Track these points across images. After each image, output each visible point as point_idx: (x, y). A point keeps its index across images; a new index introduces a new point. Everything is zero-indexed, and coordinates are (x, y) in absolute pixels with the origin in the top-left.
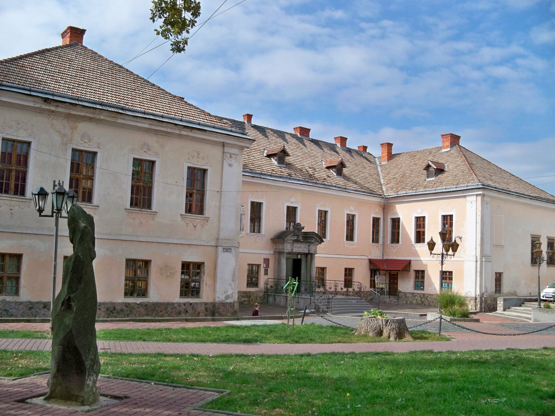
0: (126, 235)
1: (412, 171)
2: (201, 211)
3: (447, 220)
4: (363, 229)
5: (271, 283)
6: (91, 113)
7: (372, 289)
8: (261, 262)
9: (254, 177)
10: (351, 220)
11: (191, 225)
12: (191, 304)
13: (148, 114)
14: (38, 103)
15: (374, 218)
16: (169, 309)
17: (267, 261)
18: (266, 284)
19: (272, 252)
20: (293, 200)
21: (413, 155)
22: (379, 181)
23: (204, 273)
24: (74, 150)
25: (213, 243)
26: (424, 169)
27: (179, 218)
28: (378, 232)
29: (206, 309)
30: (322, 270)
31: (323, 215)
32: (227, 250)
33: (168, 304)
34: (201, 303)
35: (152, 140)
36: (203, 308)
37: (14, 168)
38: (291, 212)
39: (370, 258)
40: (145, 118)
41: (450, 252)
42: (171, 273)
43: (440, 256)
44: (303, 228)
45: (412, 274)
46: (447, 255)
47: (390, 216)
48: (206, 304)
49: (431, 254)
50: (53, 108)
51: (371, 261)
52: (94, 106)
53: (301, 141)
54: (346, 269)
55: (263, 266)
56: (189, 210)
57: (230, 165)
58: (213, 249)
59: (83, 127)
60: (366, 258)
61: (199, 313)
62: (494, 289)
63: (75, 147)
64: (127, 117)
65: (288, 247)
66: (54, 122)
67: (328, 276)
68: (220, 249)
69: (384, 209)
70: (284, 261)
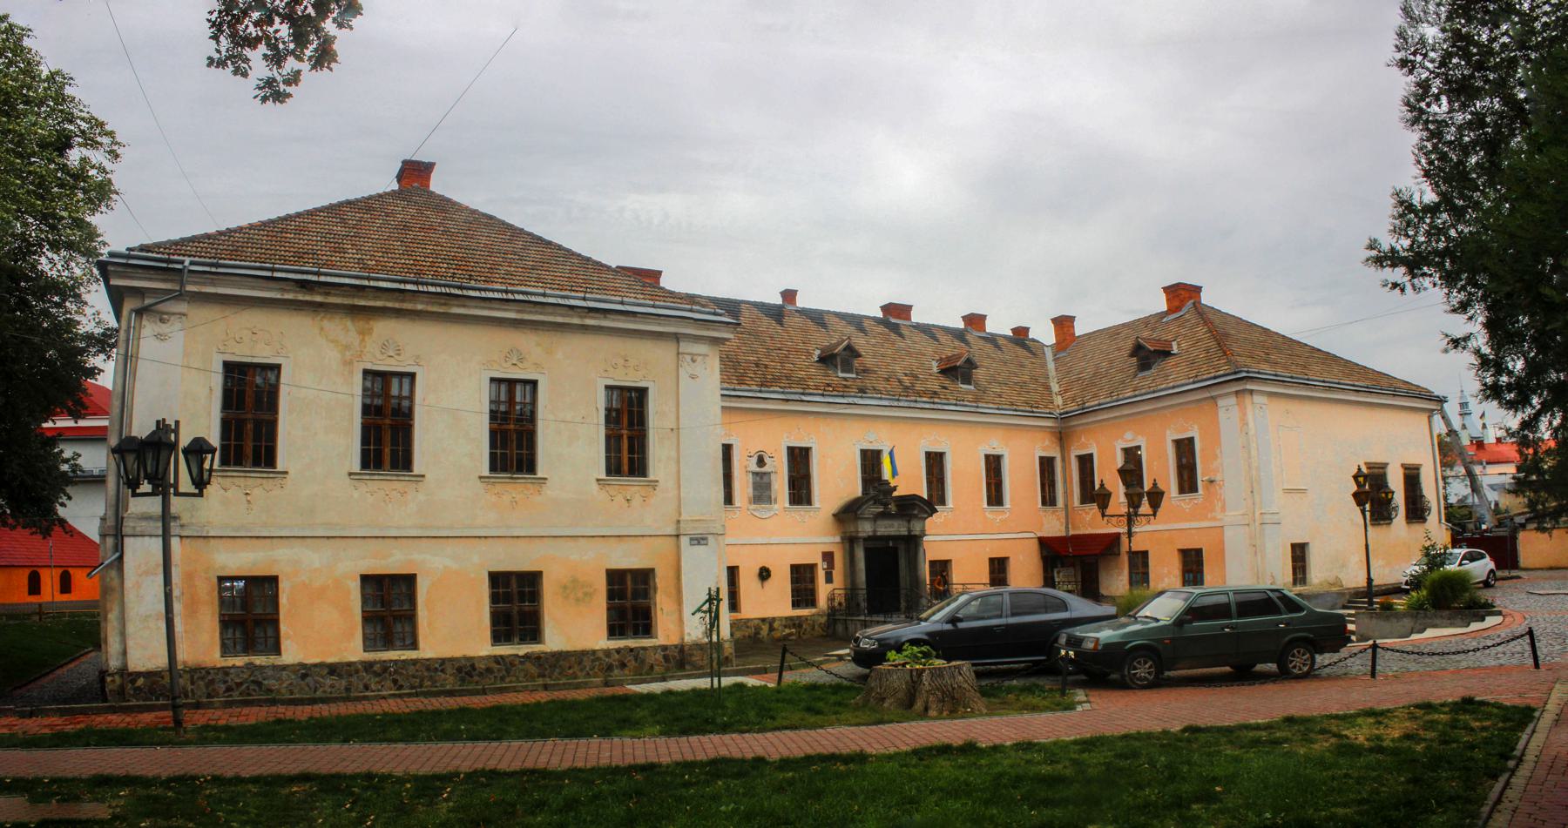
0: (484, 527)
1: (1111, 361)
2: (638, 467)
3: (1185, 448)
4: (1020, 478)
5: (840, 597)
6: (397, 300)
8: (817, 559)
10: (994, 465)
11: (619, 498)
12: (632, 650)
13: (513, 292)
14: (288, 291)
15: (1041, 458)
16: (587, 663)
17: (828, 557)
18: (831, 599)
19: (838, 539)
21: (1113, 333)
22: (1048, 388)
23: (655, 589)
24: (366, 372)
25: (671, 530)
26: (1132, 355)
27: (595, 486)
28: (1052, 484)
29: (666, 658)
30: (941, 568)
31: (935, 462)
32: (699, 540)
33: (584, 653)
34: (655, 648)
35: (528, 342)
36: (659, 656)
37: (249, 416)
40: (508, 300)
41: (1145, 508)
42: (586, 594)
43: (1125, 519)
44: (895, 489)
45: (1125, 559)
46: (1136, 514)
47: (1076, 451)
48: (665, 648)
49: (1103, 515)
50: (318, 299)
51: (1044, 543)
52: (402, 286)
53: (895, 329)
54: (992, 560)
56: (613, 468)
57: (693, 377)
58: (672, 540)
59: (384, 328)
61: (652, 667)
62: (1290, 579)
63: (369, 366)
64: (468, 303)
65: (866, 528)
66: (326, 324)
67: (957, 576)
68: (684, 541)
69: (1061, 439)
70: (860, 554)
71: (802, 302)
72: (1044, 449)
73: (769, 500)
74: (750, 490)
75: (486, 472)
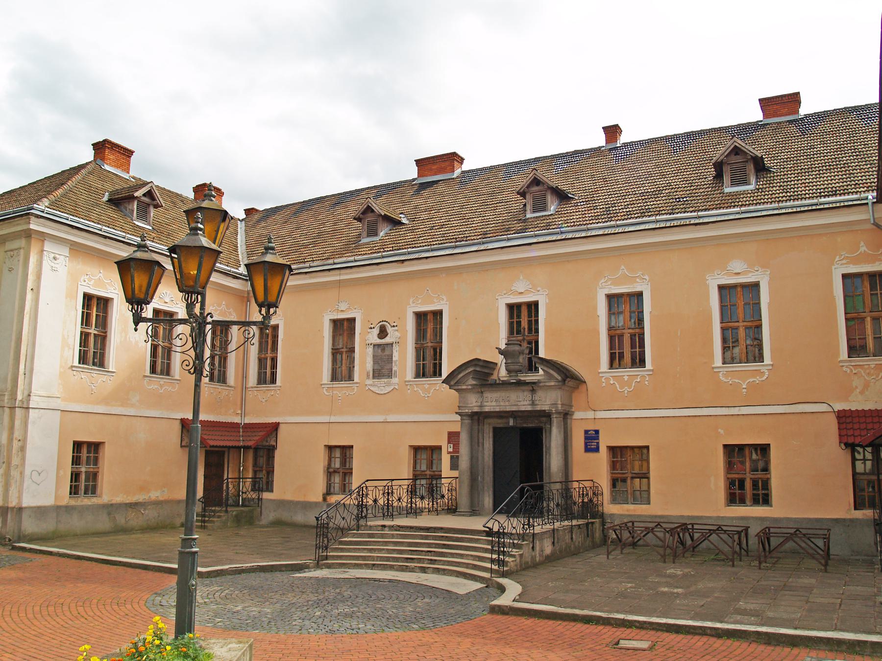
7: (867, 514)
8: (443, 442)
9: (403, 261)
10: (740, 300)
20: (521, 286)
38: (523, 316)
39: (838, 407)
54: (733, 451)
55: (446, 449)
60: (823, 408)
65: (473, 403)
71: (624, 138)
72: (855, 261)
73: (390, 375)
74: (369, 366)
75: (76, 363)
